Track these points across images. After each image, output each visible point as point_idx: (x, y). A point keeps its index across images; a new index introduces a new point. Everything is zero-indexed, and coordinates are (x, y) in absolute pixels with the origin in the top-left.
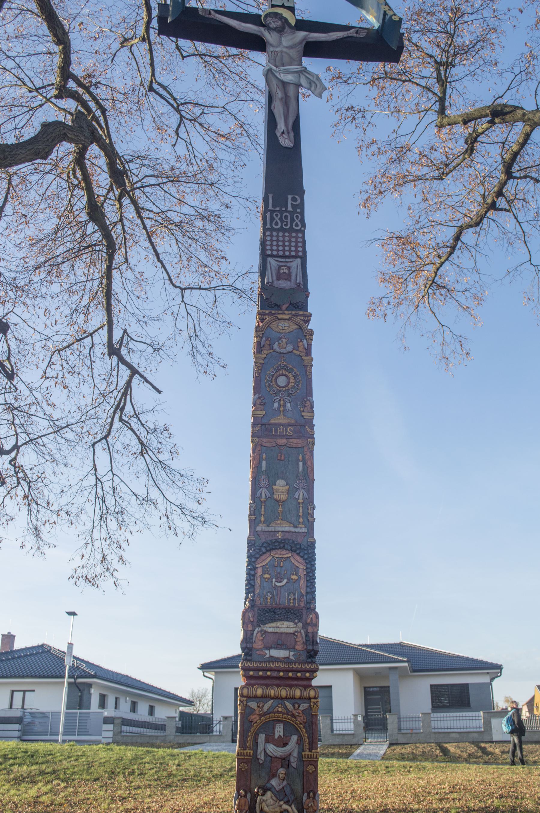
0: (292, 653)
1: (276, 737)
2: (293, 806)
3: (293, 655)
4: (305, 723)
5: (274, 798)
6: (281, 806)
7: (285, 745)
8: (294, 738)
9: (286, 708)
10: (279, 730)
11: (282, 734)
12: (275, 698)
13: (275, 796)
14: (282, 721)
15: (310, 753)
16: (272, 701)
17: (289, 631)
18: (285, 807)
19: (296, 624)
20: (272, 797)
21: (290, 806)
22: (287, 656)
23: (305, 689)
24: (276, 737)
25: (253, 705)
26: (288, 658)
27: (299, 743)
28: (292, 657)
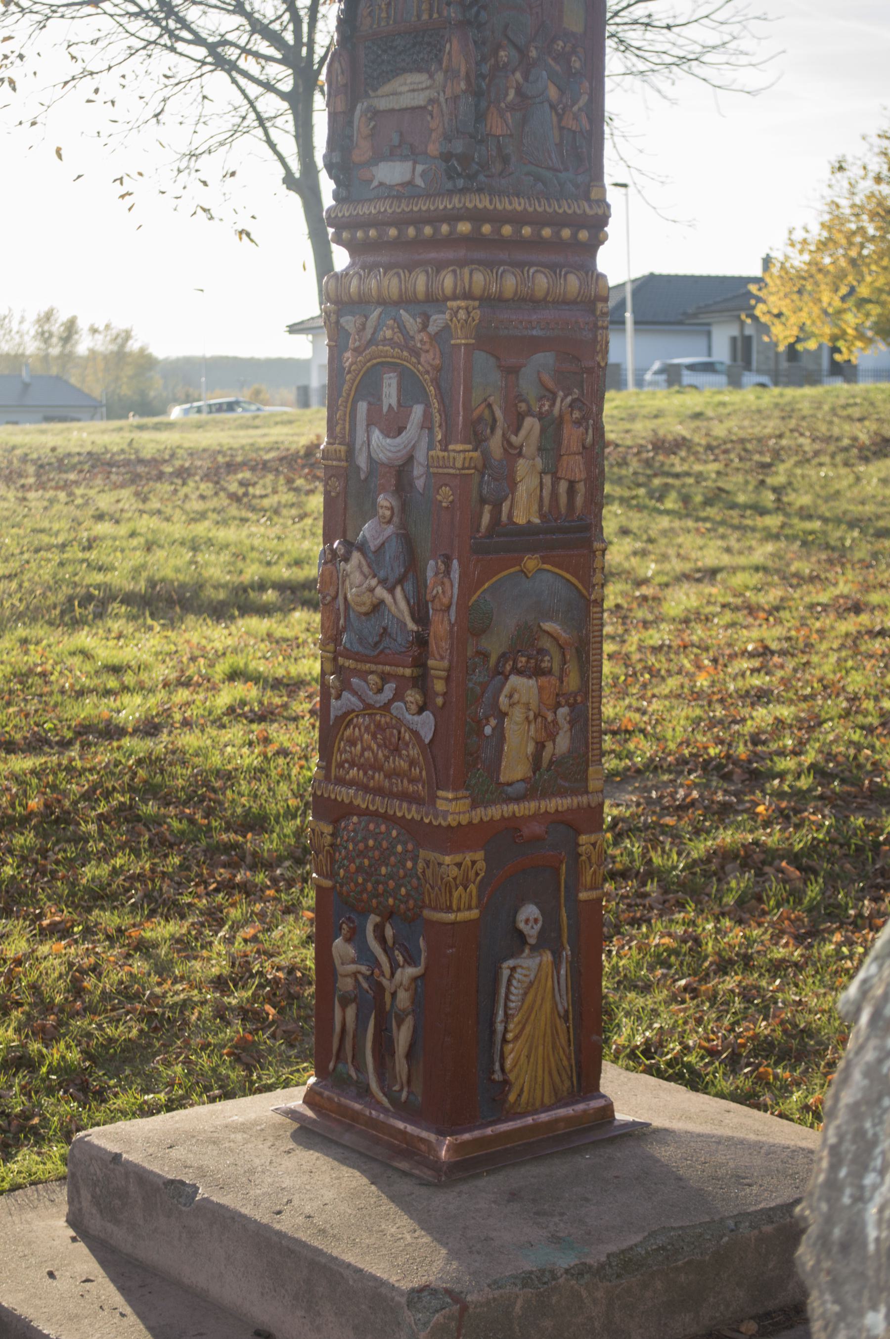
0: (420, 168)
1: (385, 409)
2: (398, 590)
3: (423, 174)
4: (439, 369)
5: (366, 569)
6: (372, 590)
7: (400, 430)
8: (418, 411)
9: (401, 327)
10: (390, 391)
11: (394, 401)
12: (382, 302)
13: (369, 566)
14: (393, 367)
15: (441, 454)
16: (379, 310)
17: (415, 103)
18: (381, 592)
19: (431, 76)
20: (360, 566)
21: (391, 591)
22: (407, 177)
23: (438, 272)
24: (385, 409)
25: (349, 322)
26: (410, 183)
27: (427, 424)
28: (419, 182)
